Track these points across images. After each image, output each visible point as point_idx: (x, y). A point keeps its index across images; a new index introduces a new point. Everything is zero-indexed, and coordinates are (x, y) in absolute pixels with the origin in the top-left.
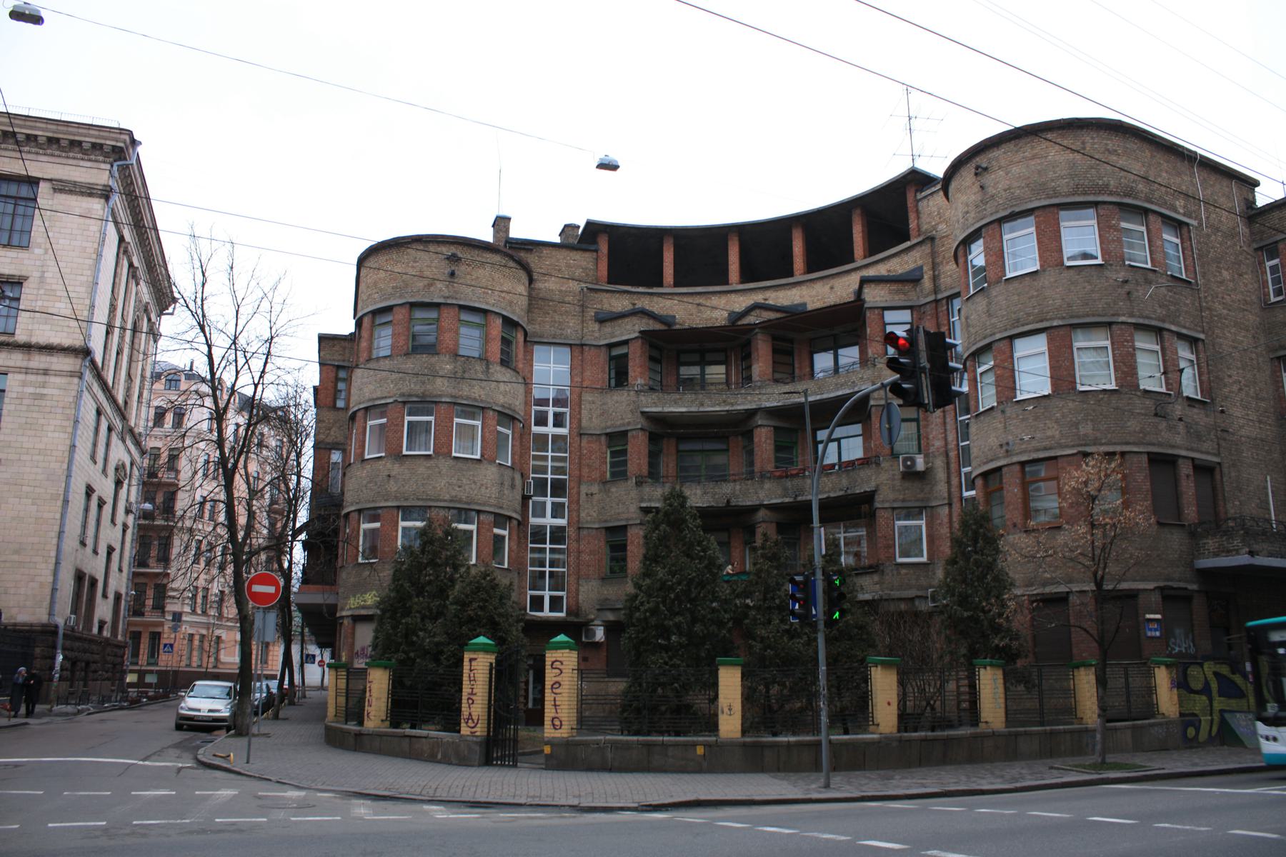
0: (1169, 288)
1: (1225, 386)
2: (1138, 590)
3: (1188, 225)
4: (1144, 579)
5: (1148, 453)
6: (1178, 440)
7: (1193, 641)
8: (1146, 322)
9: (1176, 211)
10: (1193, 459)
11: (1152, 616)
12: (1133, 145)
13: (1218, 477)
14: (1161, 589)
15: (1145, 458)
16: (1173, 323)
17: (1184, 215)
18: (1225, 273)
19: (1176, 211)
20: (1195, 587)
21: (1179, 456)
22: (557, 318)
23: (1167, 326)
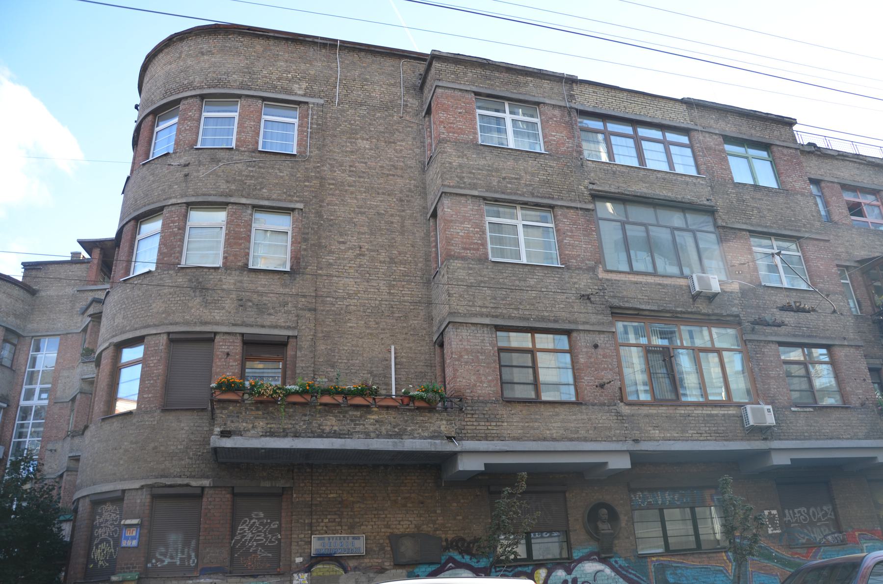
0: (249, 164)
1: (331, 252)
2: (124, 491)
3: (307, 103)
4: (132, 478)
5: (169, 333)
6: (218, 315)
7: (197, 550)
8: (200, 199)
9: (291, 92)
10: (243, 335)
11: (128, 522)
12: (234, 42)
13: (290, 352)
14: (151, 487)
15: (164, 339)
16: (243, 196)
17: (304, 95)
18: (366, 144)
19: (291, 92)
20: (206, 483)
21: (215, 333)
23: (232, 200)
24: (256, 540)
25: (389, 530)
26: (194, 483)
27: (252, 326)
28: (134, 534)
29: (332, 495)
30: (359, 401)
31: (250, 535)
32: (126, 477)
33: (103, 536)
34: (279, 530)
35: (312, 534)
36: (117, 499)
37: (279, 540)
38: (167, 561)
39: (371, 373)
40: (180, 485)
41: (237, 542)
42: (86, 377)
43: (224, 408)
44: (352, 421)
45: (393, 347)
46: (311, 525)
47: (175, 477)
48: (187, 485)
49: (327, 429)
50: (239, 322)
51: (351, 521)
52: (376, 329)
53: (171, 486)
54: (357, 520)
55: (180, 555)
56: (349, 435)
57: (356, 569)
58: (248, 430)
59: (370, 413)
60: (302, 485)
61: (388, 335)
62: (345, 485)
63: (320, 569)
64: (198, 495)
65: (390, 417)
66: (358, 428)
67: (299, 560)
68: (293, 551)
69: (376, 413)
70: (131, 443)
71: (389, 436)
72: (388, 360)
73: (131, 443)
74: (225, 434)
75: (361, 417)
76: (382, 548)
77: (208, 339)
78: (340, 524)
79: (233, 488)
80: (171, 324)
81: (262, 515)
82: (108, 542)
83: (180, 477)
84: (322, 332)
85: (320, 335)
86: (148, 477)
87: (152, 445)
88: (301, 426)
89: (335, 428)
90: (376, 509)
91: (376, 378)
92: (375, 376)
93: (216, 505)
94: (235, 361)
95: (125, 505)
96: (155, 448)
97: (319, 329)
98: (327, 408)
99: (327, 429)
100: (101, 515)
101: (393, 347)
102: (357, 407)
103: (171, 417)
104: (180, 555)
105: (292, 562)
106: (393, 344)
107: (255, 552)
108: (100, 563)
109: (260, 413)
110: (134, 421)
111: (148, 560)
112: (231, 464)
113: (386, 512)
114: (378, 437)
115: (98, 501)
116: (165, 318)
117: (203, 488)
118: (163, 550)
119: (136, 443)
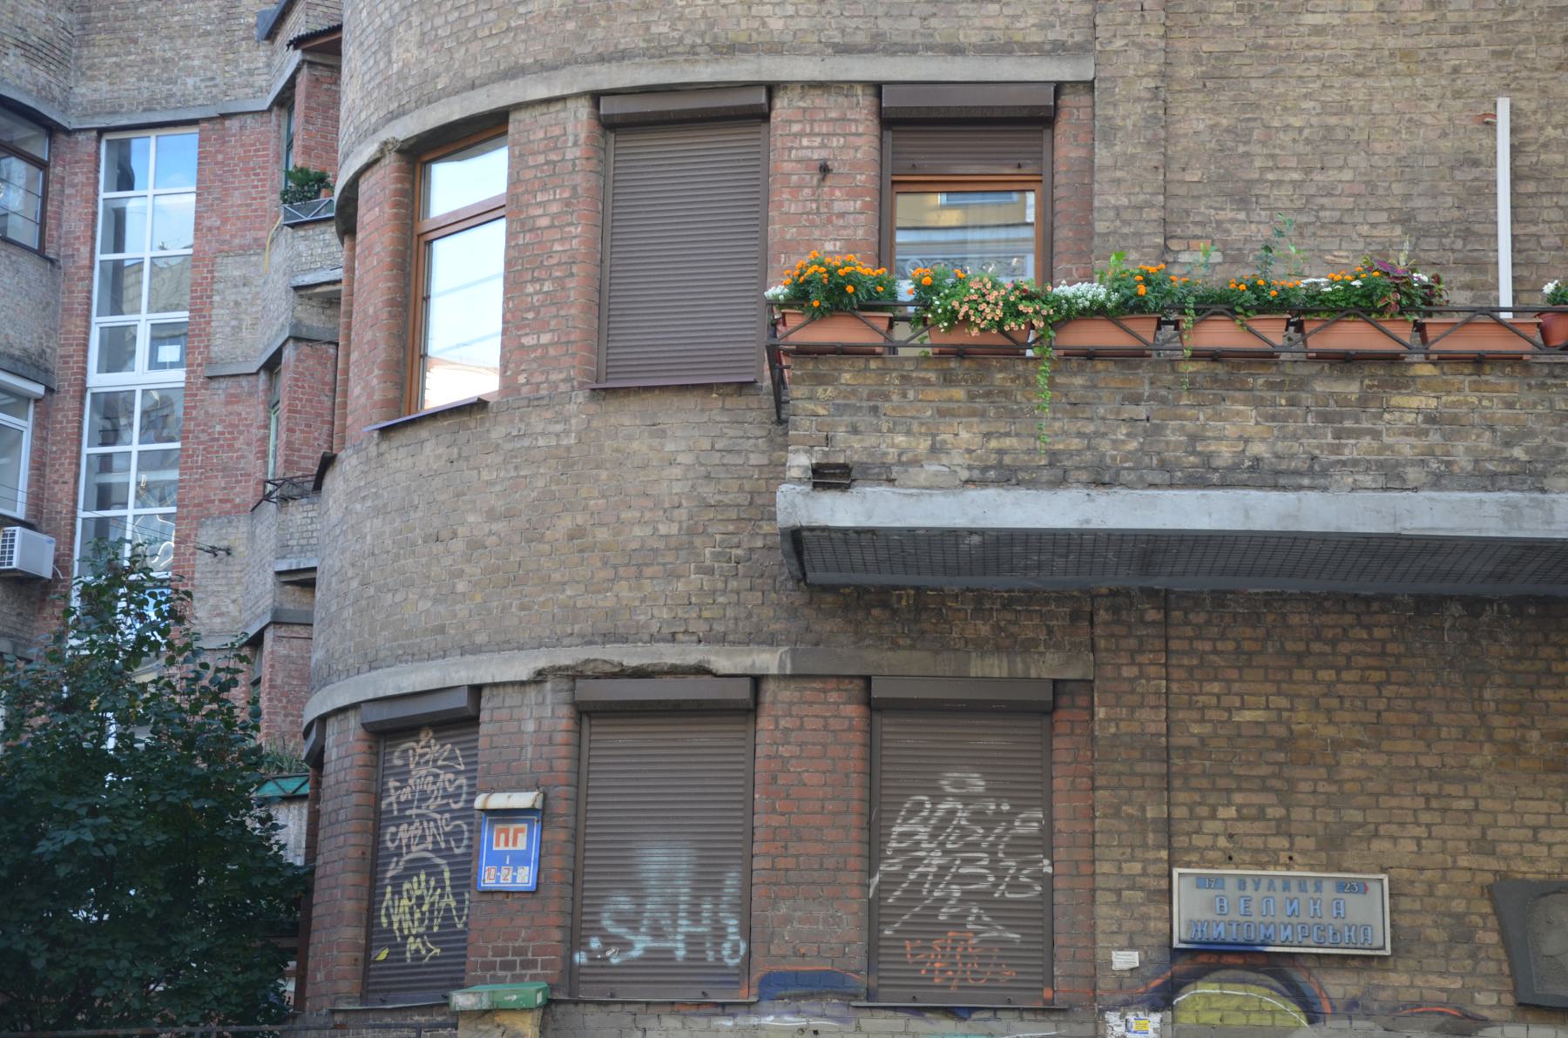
2: (476, 690)
4: (504, 645)
5: (596, 97)
10: (877, 87)
11: (499, 801)
13: (1066, 146)
14: (573, 675)
20: (767, 661)
21: (771, 88)
22: (160, 49)
24: (959, 879)
25: (1493, 864)
26: (722, 662)
27: (911, 50)
28: (522, 845)
29: (1248, 716)
30: (1353, 336)
31: (937, 859)
32: (481, 638)
33: (416, 852)
34: (1045, 842)
35: (1171, 863)
36: (457, 719)
37: (1048, 881)
38: (641, 944)
39: (1405, 220)
40: (675, 671)
41: (891, 881)
42: (308, 279)
43: (820, 380)
44: (1325, 418)
45: (1503, 106)
46: (1167, 827)
47: (653, 639)
48: (701, 670)
49: (1225, 453)
50: (861, 38)
51: (1330, 817)
52: (1430, 28)
53: (640, 673)
54: (1355, 816)
55: (685, 926)
56: (1315, 474)
57: (1352, 1007)
58: (916, 462)
59: (1403, 384)
60: (1127, 672)
61: (1483, 53)
62: (1301, 675)
63: (1206, 998)
64: (743, 706)
65: (1491, 400)
66: (1353, 449)
67: (1124, 960)
68: (1102, 925)
69: (1428, 384)
70: (491, 515)
71: (1487, 480)
72: (1482, 162)
73: (491, 515)
74: (829, 477)
75: (1363, 402)
76: (1462, 934)
77: (745, 113)
78: (1283, 828)
79: (868, 679)
80: (602, 59)
81: (977, 784)
82: (433, 871)
83: (673, 638)
84: (1197, 58)
85: (1188, 72)
86: (557, 642)
87: (565, 523)
88: (1120, 443)
89: (1258, 449)
90: (1432, 776)
91: (1431, 243)
92: (1422, 233)
93: (806, 740)
94: (853, 194)
95: (483, 742)
96: (575, 534)
97: (1183, 46)
98: (1220, 369)
99: (1225, 453)
100: (403, 775)
101: (1503, 106)
102: (1346, 361)
103: (626, 417)
104: (685, 926)
105: (1096, 967)
106: (1506, 89)
107: (958, 921)
108: (413, 945)
109: (959, 393)
110: (497, 433)
111: (575, 940)
112: (852, 587)
113: (1475, 789)
114: (1437, 482)
115: (391, 729)
116: (579, 37)
117: (757, 680)
118: (623, 903)
119: (509, 515)
